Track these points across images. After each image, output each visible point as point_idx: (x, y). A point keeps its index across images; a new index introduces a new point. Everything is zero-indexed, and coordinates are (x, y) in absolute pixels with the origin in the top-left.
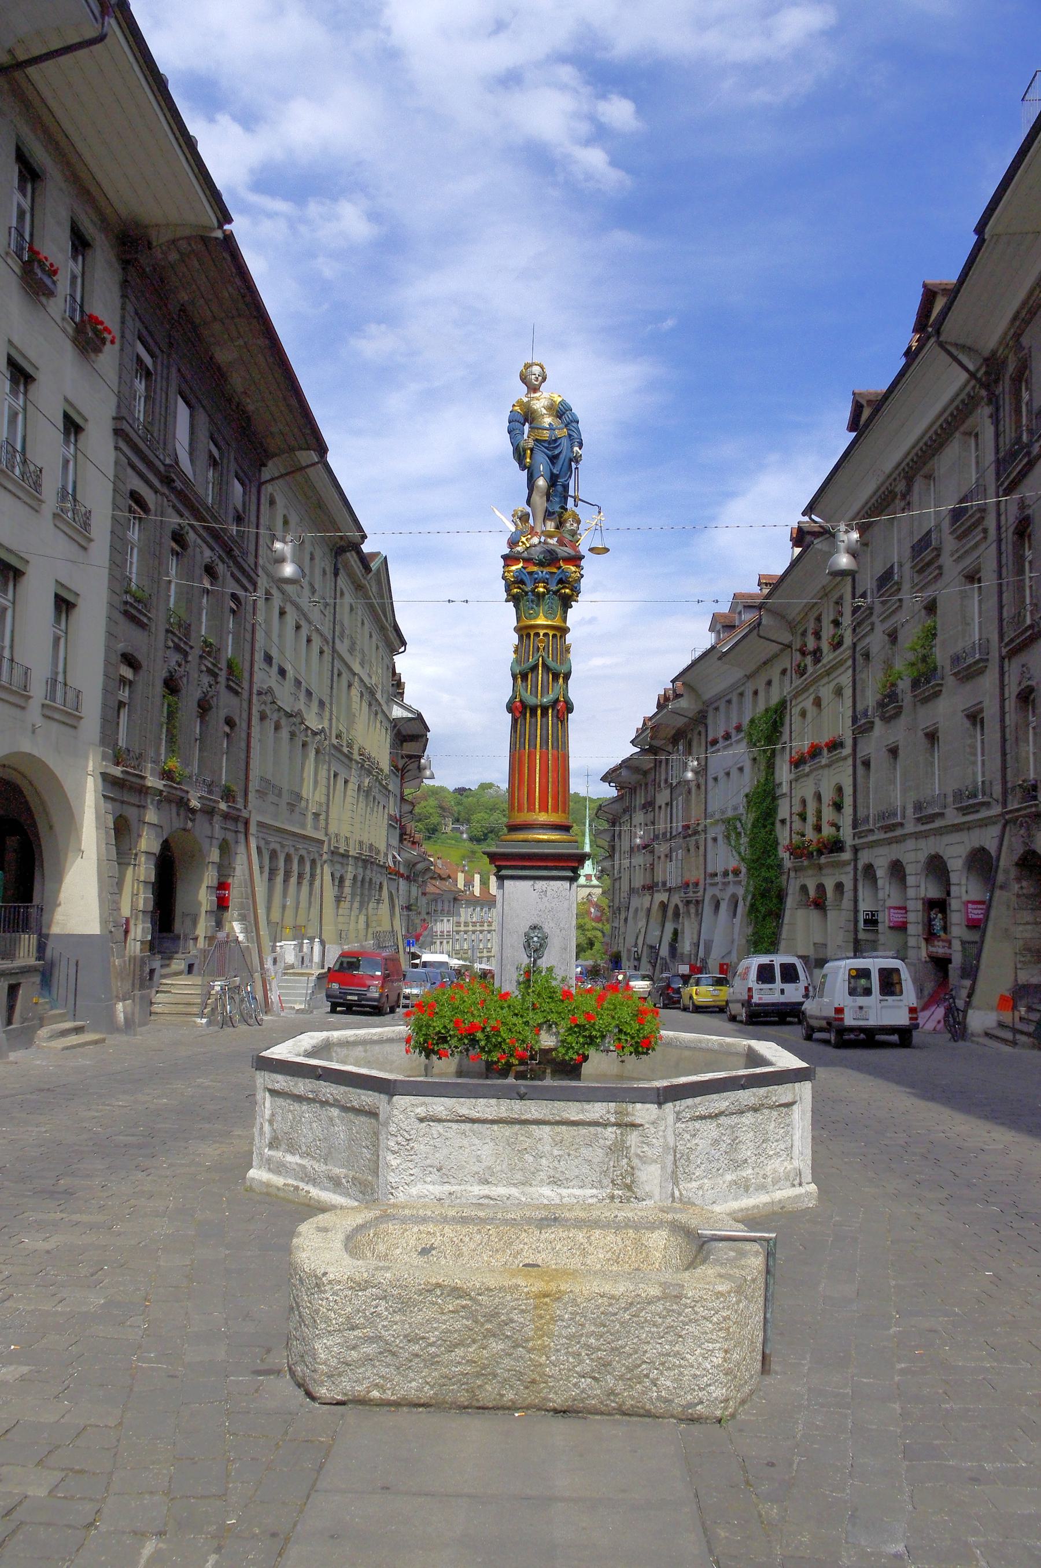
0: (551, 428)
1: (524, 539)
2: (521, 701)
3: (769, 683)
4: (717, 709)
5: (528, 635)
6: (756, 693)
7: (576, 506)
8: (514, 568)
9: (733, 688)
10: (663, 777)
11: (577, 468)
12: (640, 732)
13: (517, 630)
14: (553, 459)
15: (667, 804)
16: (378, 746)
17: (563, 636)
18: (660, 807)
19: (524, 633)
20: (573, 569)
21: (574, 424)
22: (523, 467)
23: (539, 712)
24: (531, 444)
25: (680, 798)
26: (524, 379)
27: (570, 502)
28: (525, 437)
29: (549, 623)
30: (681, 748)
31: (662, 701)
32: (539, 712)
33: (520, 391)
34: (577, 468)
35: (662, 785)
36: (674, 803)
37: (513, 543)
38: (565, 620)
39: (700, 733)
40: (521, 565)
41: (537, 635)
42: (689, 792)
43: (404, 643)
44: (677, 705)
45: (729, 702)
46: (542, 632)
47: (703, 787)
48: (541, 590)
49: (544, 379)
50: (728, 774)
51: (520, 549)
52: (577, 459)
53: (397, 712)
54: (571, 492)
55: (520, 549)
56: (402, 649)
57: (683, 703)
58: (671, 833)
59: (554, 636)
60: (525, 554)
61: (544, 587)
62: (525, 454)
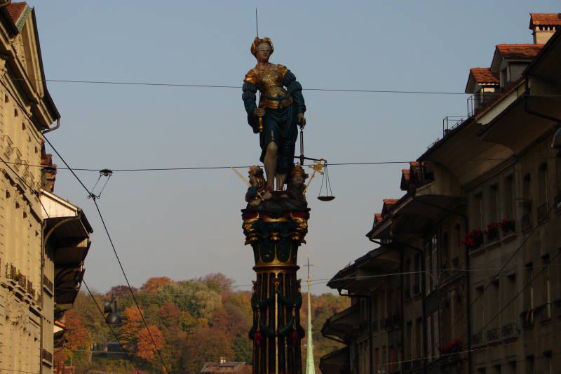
0: (279, 99)
1: (259, 194)
2: (261, 331)
3: (544, 167)
4: (479, 196)
5: (265, 275)
6: (527, 178)
7: (302, 163)
8: (252, 220)
9: (494, 172)
10: (412, 284)
11: (302, 132)
12: (378, 223)
13: (254, 269)
14: (281, 125)
15: (419, 320)
16: (32, 262)
17: (295, 275)
18: (410, 324)
19: (262, 272)
20: (301, 220)
21: (298, 93)
22: (256, 131)
23: (277, 338)
24: (262, 113)
25: (436, 314)
26: (254, 52)
27: (297, 161)
28: (257, 102)
29: (284, 265)
30: (434, 241)
31: (407, 177)
32: (277, 338)
33: (253, 62)
34: (302, 132)
35: (412, 295)
36: (429, 319)
37: (250, 197)
38: (295, 260)
39: (458, 227)
40: (258, 217)
41: (274, 274)
42: (447, 305)
43: (55, 115)
44: (426, 192)
45: (495, 187)
46: (277, 273)
47: (465, 300)
48: (275, 238)
49: (271, 51)
50: (496, 283)
51: (256, 202)
52: (303, 123)
53: (51, 209)
54: (297, 153)
55: (256, 202)
56: (55, 124)
57: (434, 189)
58: (426, 361)
59: (287, 275)
60: (260, 208)
61: (277, 236)
62: (258, 120)
